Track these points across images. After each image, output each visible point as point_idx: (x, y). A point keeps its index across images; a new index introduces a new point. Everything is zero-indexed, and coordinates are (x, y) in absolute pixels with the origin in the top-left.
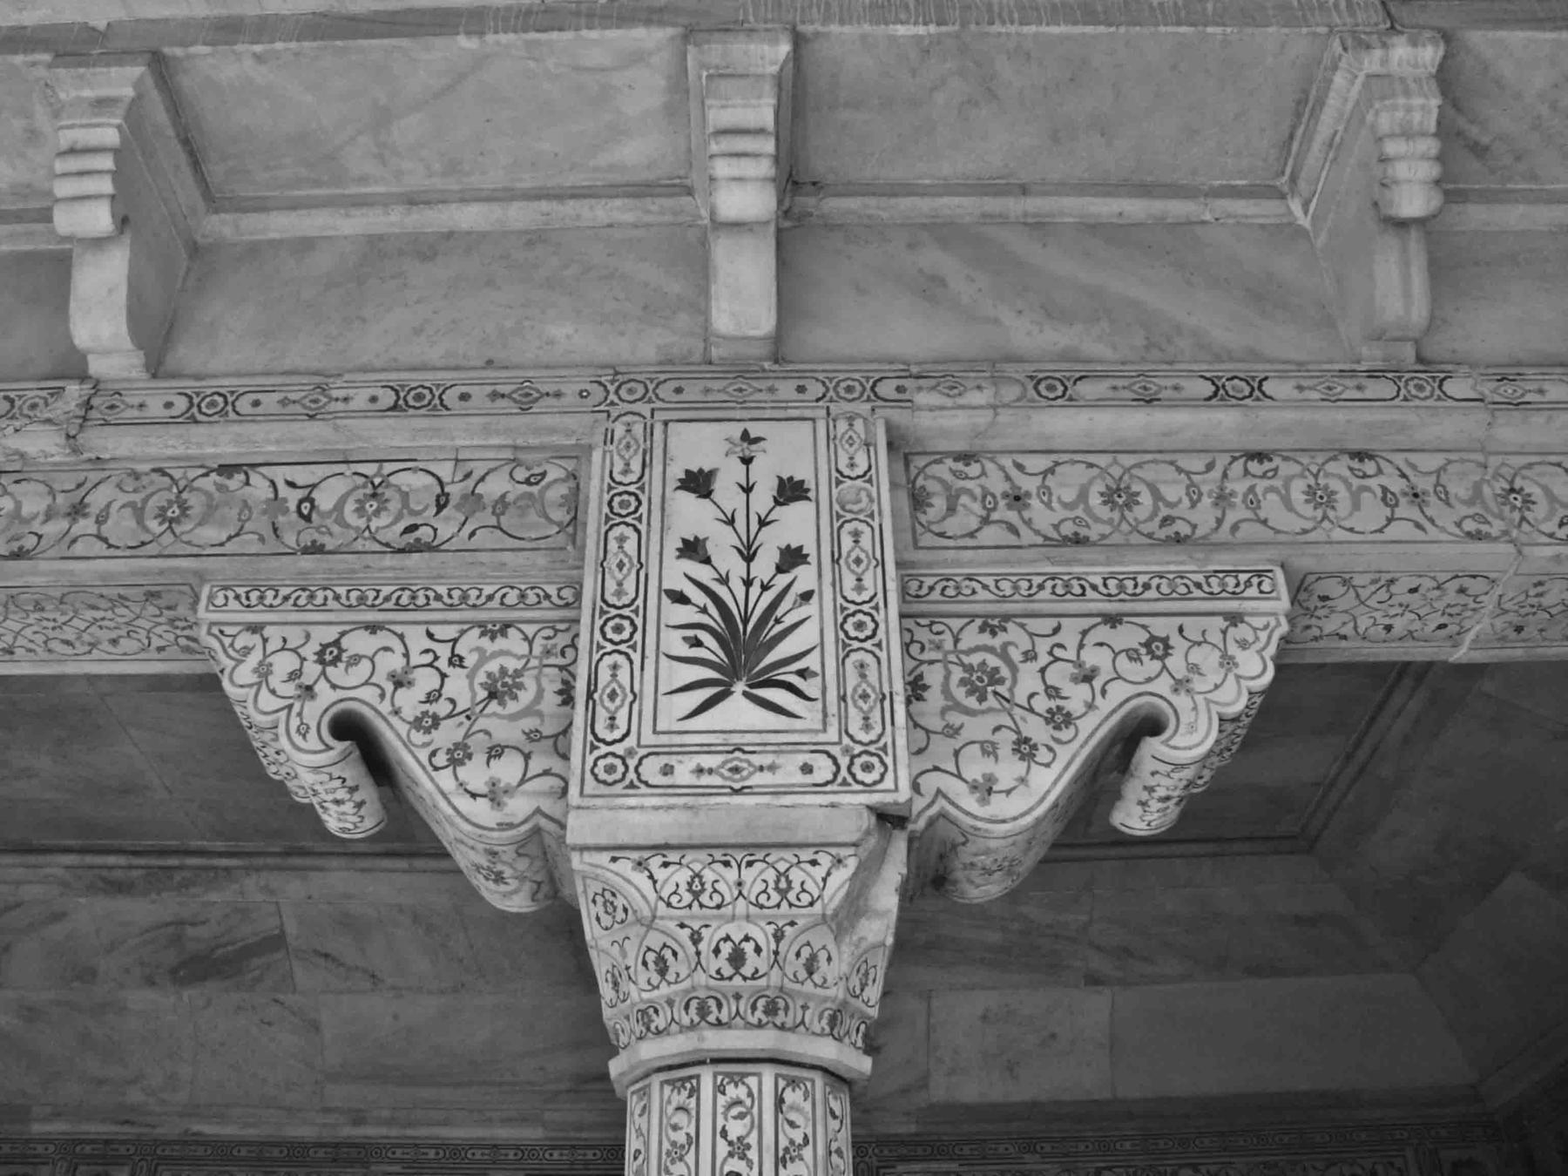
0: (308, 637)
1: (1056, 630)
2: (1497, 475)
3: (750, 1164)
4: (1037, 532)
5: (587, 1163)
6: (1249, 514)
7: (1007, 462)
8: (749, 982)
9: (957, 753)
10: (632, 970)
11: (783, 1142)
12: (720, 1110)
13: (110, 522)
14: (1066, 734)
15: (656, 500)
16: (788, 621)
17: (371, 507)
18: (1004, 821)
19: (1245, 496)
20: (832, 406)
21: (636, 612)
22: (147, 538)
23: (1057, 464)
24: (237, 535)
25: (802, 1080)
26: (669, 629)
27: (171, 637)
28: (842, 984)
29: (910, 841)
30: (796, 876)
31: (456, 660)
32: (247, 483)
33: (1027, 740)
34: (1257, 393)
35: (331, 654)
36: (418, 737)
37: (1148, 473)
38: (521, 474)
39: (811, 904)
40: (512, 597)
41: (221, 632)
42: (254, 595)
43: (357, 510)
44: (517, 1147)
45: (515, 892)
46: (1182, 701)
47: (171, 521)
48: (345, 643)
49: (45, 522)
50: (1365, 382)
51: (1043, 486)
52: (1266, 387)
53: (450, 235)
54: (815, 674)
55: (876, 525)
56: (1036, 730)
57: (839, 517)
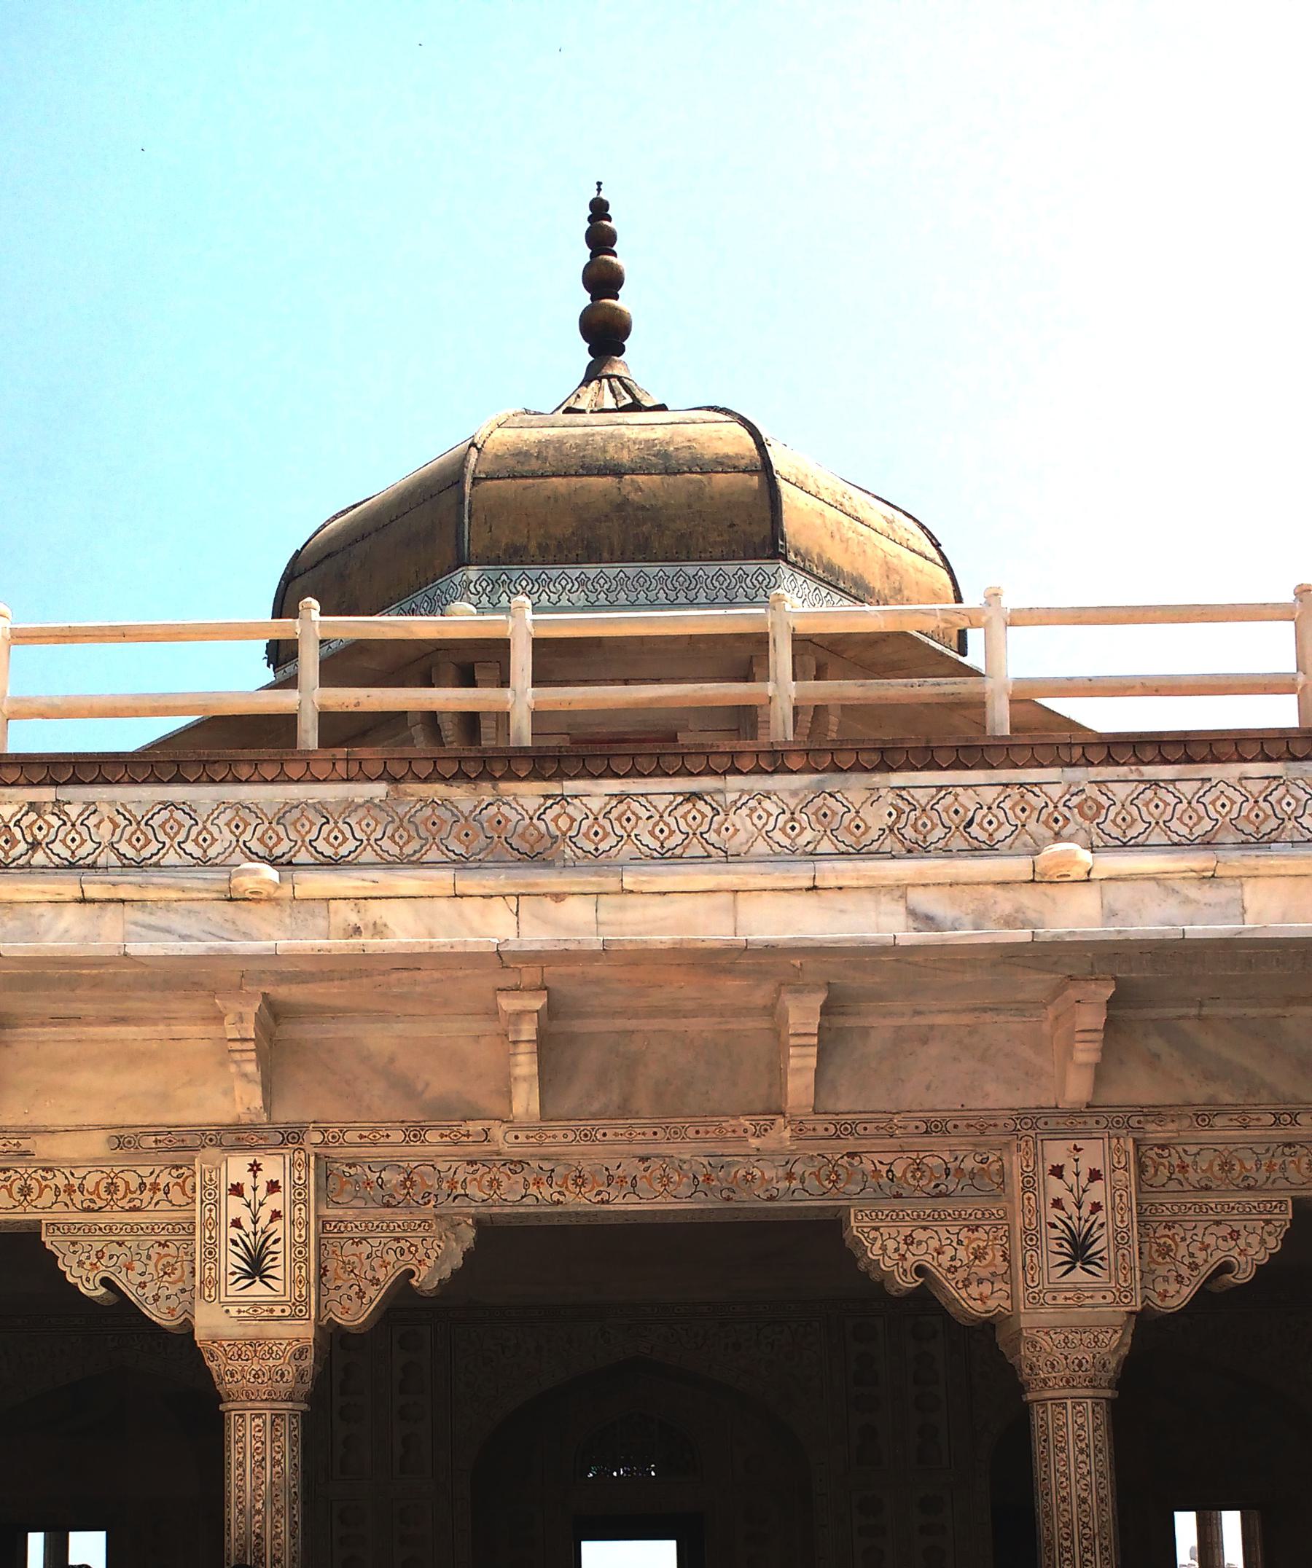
7: (1180, 1149)
17: (918, 1174)
31: (960, 1242)
35: (909, 1240)
36: (950, 1276)
37: (1240, 1154)
38: (978, 1158)
40: (979, 1216)
46: (1242, 1259)
53: (932, 1027)
56: (1185, 1271)
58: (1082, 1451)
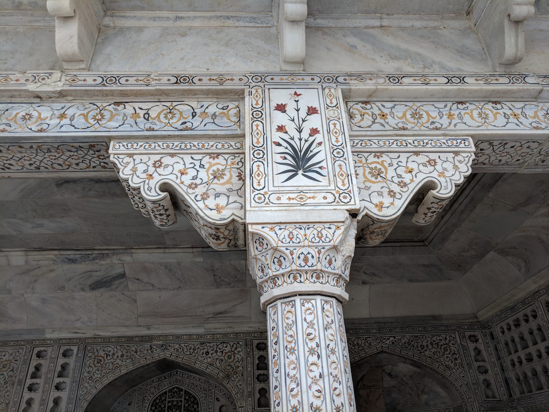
0: (149, 158)
1: (399, 157)
2: (542, 109)
3: (315, 330)
4: (390, 126)
6: (460, 121)
7: (379, 104)
8: (311, 268)
9: (370, 195)
10: (269, 265)
11: (325, 323)
12: (303, 312)
13: (75, 120)
14: (405, 189)
15: (268, 113)
16: (315, 151)
17: (170, 116)
18: (387, 217)
19: (458, 115)
20: (323, 85)
21: (264, 148)
22: (89, 125)
23: (395, 105)
24: (123, 125)
25: (329, 301)
26: (275, 154)
27: (98, 162)
28: (340, 268)
29: (358, 222)
30: (324, 232)
31: (202, 166)
32: (125, 108)
33: (392, 191)
34: (462, 81)
36: (190, 191)
38: (220, 106)
39: (330, 242)
40: (220, 146)
41: (118, 157)
42: (129, 145)
43: (165, 117)
44: (197, 335)
45: (222, 243)
46: (442, 179)
47: (98, 120)
48: (162, 161)
49: (51, 119)
50: (498, 78)
51: (391, 112)
52: (465, 79)
53: (190, 28)
54: (325, 168)
55: (341, 121)
56: (396, 188)
57: (328, 119)
58: (312, 351)
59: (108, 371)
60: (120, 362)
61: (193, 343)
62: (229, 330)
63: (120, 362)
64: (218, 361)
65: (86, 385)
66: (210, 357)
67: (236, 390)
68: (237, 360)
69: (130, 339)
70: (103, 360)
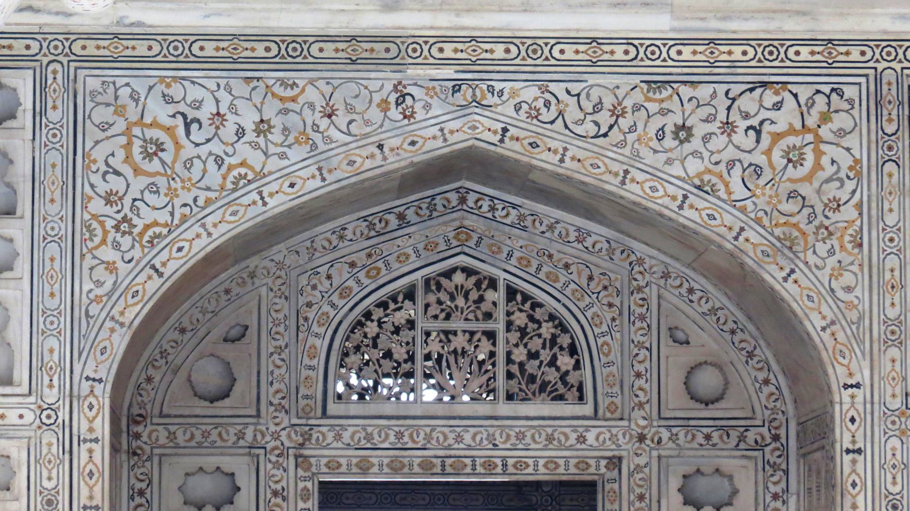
5: (733, 65)
44: (629, 41)
59: (203, 196)
60: (255, 159)
61: (610, 81)
62: (794, 27)
63: (255, 159)
64: (737, 171)
65: (108, 254)
66: (695, 153)
67: (825, 309)
68: (830, 170)
69: (292, 50)
70: (169, 145)
